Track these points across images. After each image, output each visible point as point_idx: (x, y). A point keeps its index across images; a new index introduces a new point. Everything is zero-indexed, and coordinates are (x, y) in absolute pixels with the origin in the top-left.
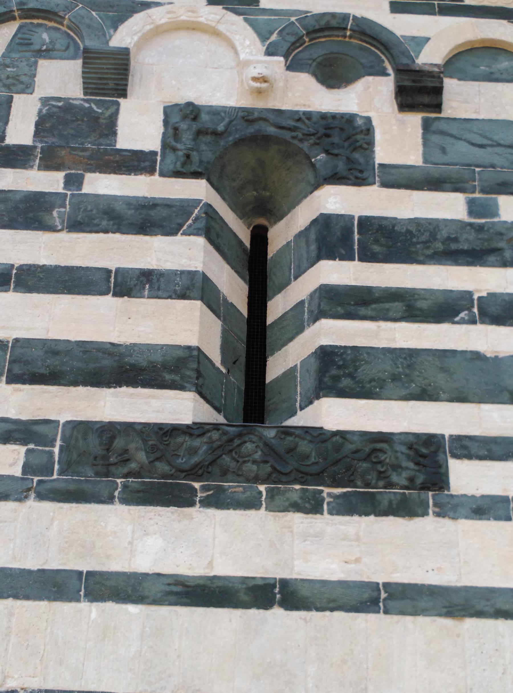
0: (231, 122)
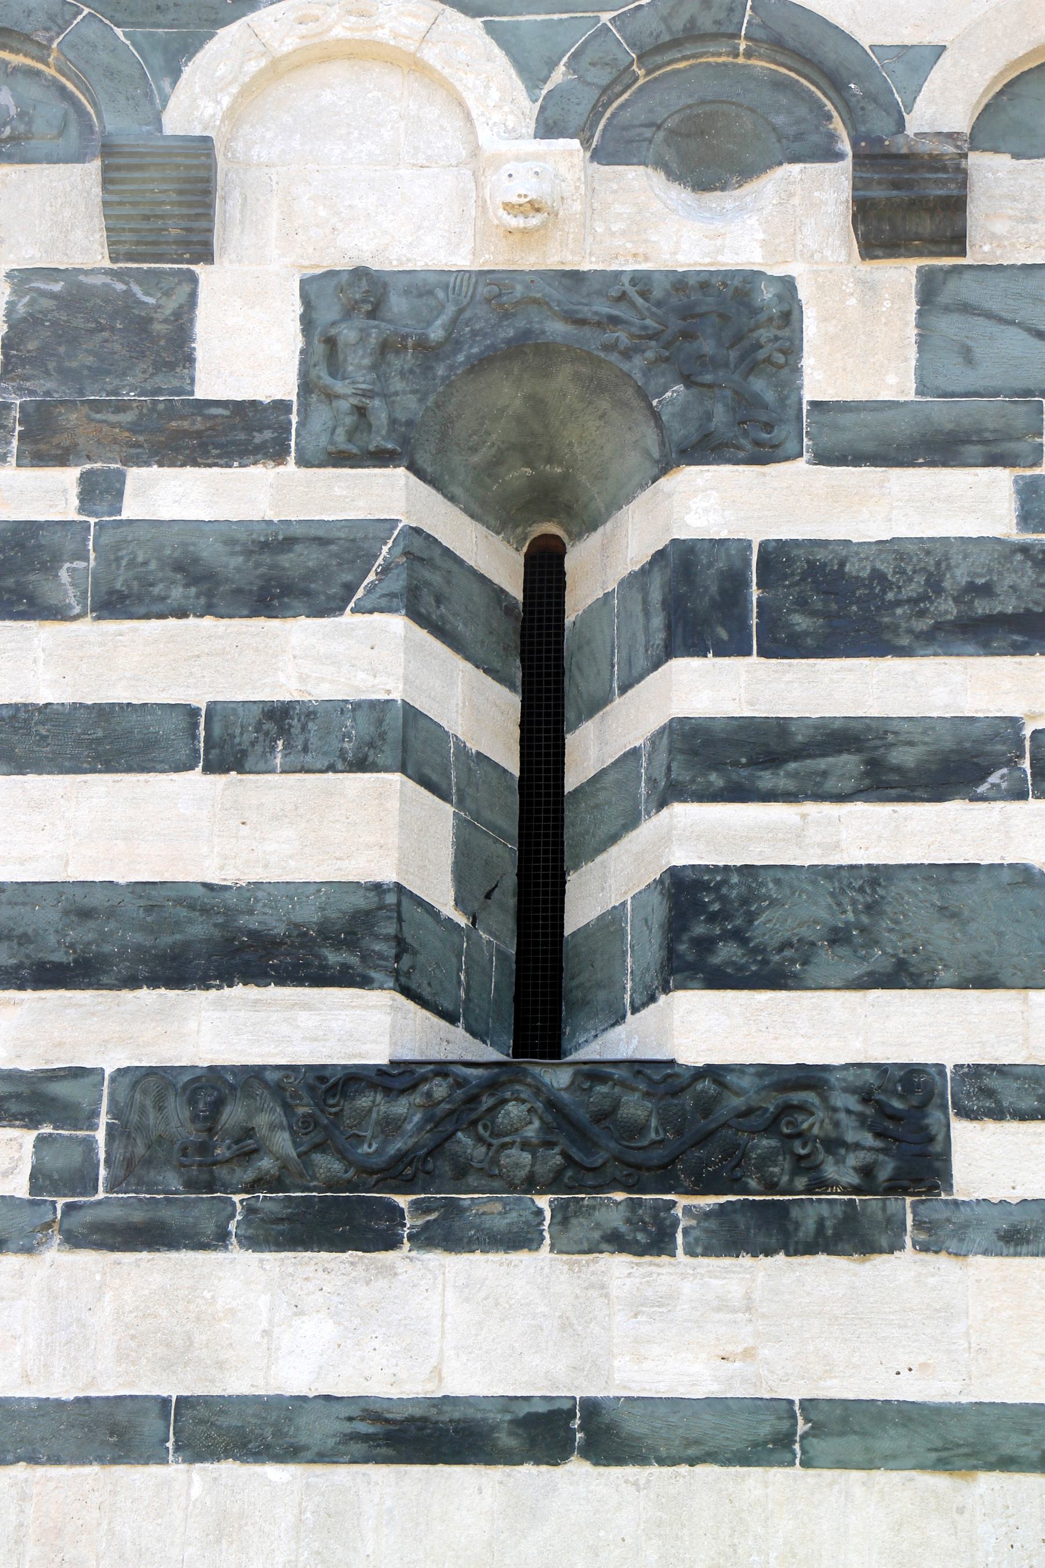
0: (461, 311)
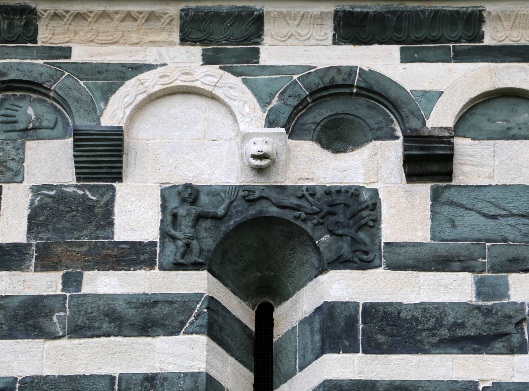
0: (232, 202)
